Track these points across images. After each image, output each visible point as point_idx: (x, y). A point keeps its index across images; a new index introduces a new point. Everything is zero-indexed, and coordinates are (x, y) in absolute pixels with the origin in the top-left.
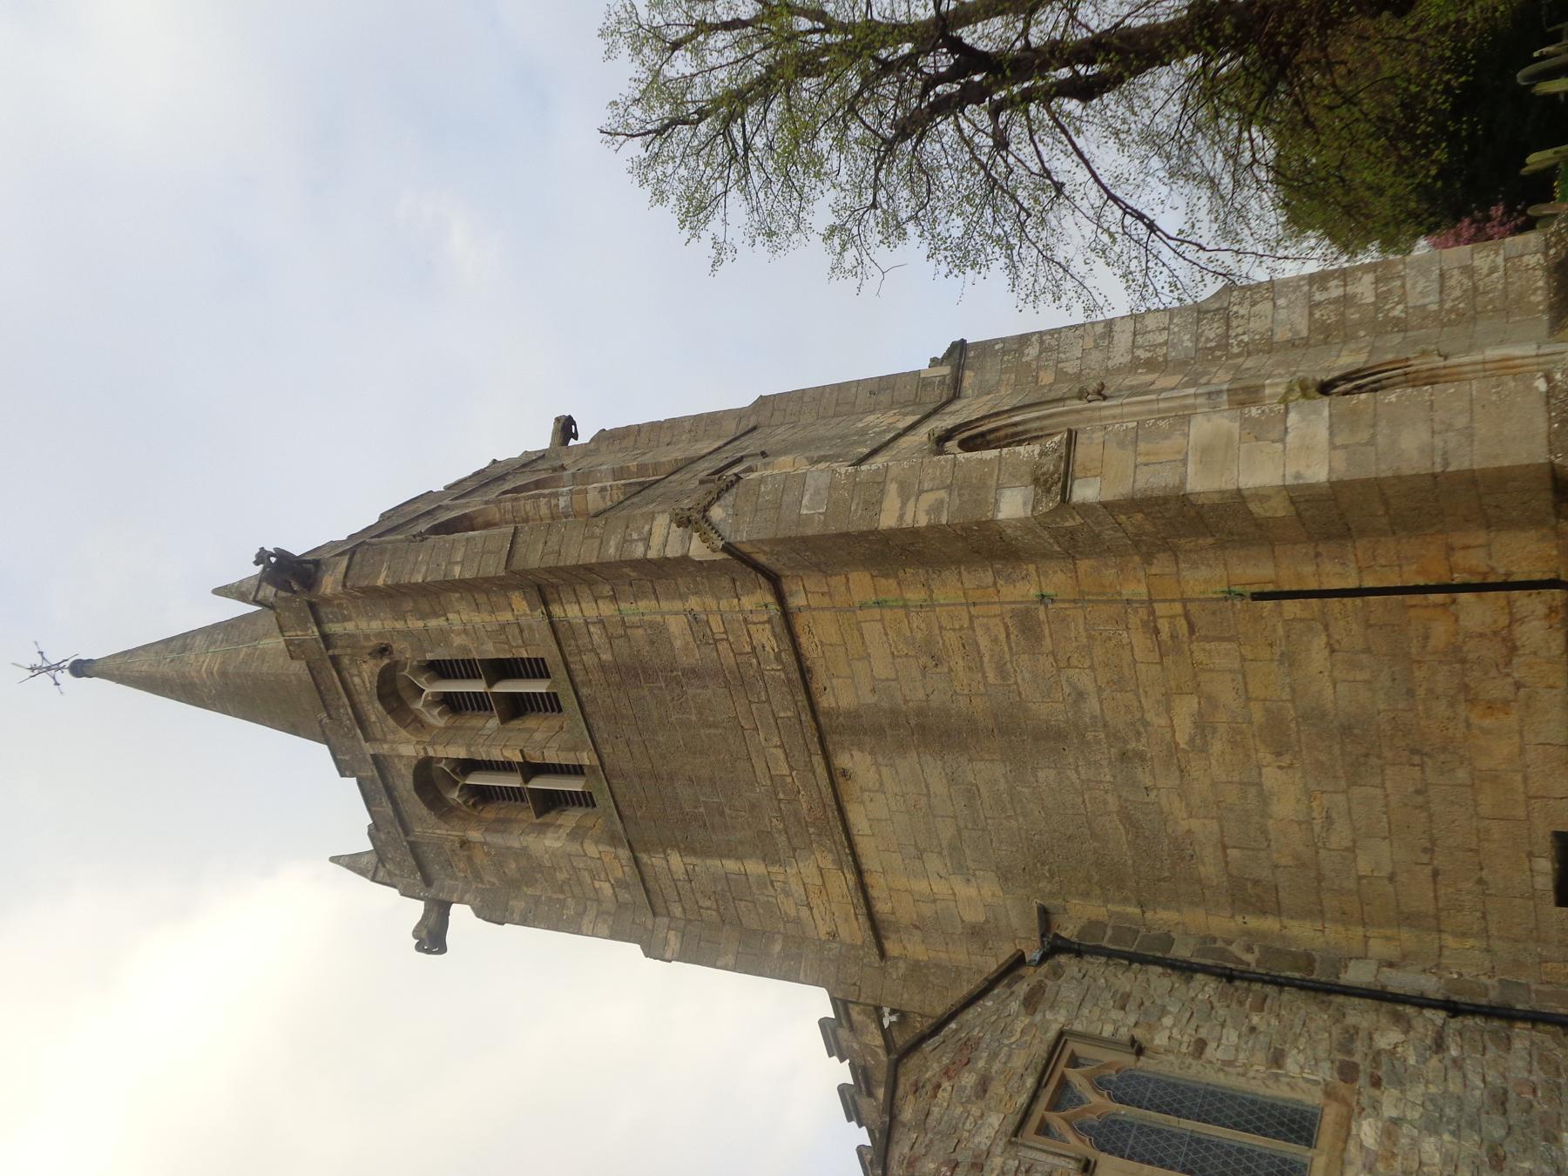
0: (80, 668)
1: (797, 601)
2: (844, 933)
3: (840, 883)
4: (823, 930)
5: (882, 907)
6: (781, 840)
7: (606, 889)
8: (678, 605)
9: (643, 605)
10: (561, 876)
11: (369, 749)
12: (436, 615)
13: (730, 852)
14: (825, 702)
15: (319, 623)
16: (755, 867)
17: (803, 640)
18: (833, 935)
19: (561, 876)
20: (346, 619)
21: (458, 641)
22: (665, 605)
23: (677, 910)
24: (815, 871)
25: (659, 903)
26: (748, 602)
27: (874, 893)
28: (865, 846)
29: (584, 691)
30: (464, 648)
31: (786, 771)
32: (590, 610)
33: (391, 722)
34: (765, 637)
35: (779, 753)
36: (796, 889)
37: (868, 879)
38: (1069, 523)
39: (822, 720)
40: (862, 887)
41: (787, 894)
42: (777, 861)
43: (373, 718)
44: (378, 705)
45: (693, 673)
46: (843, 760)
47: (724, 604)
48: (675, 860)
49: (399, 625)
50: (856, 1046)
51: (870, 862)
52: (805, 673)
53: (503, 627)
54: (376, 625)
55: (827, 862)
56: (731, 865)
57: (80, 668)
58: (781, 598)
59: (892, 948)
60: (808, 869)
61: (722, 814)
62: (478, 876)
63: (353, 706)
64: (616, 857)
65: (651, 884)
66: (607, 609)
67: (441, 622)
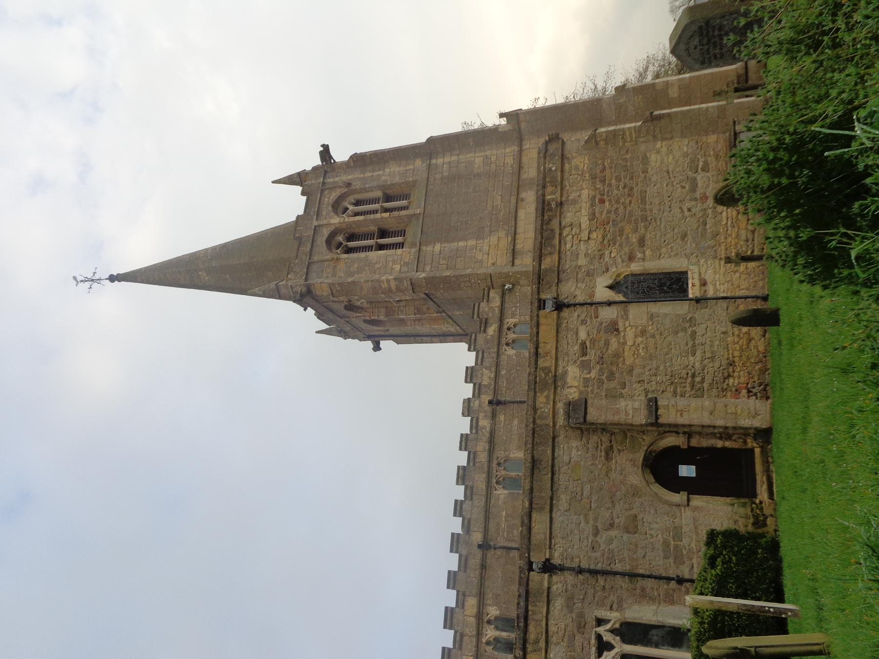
0: (112, 278)
1: (524, 147)
2: (499, 263)
3: (505, 242)
4: (490, 262)
5: (519, 246)
6: (487, 230)
7: (397, 267)
8: (482, 154)
9: (468, 155)
10: (377, 266)
11: (315, 223)
12: (380, 170)
13: (465, 239)
14: (524, 176)
15: (324, 178)
16: (471, 243)
17: (523, 158)
18: (493, 264)
19: (377, 266)
20: (337, 176)
21: (384, 178)
22: (477, 155)
23: (428, 268)
24: (496, 239)
25: (421, 266)
26: (507, 150)
27: (517, 241)
28: (520, 224)
29: (430, 187)
30: (386, 181)
31: (499, 202)
32: (447, 159)
33: (332, 213)
34: (510, 160)
35: (500, 198)
36: (486, 248)
37: (517, 237)
38: (621, 101)
39: (521, 182)
40: (514, 239)
41: (481, 251)
42: (483, 239)
43: (324, 213)
44: (330, 208)
45: (478, 175)
46: (523, 195)
47: (499, 152)
48: (438, 247)
49: (362, 176)
50: (486, 309)
51: (519, 230)
52: (520, 167)
53: (407, 170)
54: (350, 177)
55: (502, 234)
56: (461, 244)
57: (112, 278)
58: (521, 145)
59: (517, 262)
60: (493, 239)
61: (467, 224)
62: (334, 275)
63: (319, 208)
64: (410, 253)
65: (421, 259)
66: (454, 158)
67: (381, 172)
